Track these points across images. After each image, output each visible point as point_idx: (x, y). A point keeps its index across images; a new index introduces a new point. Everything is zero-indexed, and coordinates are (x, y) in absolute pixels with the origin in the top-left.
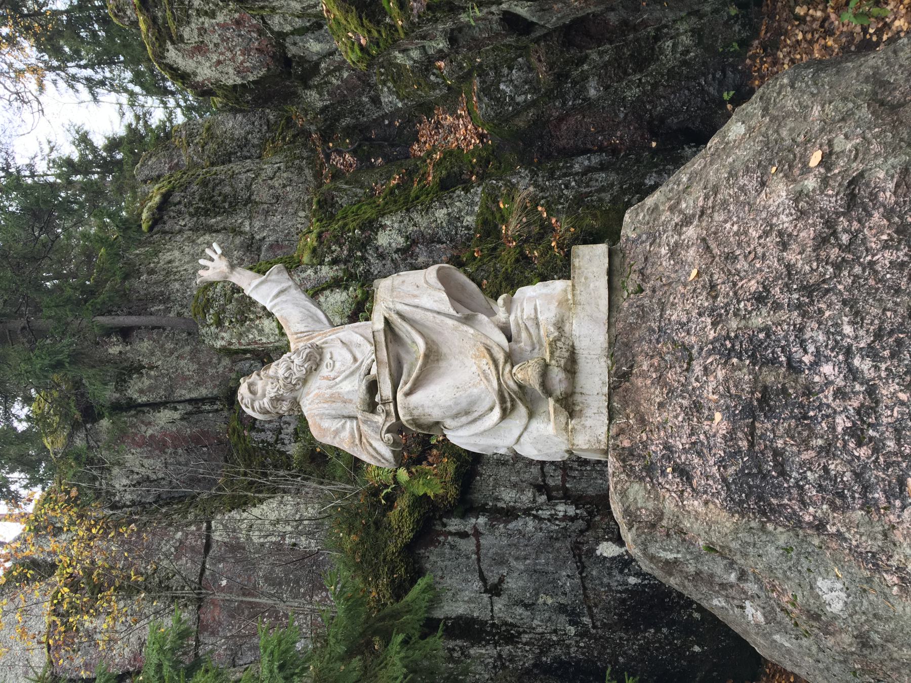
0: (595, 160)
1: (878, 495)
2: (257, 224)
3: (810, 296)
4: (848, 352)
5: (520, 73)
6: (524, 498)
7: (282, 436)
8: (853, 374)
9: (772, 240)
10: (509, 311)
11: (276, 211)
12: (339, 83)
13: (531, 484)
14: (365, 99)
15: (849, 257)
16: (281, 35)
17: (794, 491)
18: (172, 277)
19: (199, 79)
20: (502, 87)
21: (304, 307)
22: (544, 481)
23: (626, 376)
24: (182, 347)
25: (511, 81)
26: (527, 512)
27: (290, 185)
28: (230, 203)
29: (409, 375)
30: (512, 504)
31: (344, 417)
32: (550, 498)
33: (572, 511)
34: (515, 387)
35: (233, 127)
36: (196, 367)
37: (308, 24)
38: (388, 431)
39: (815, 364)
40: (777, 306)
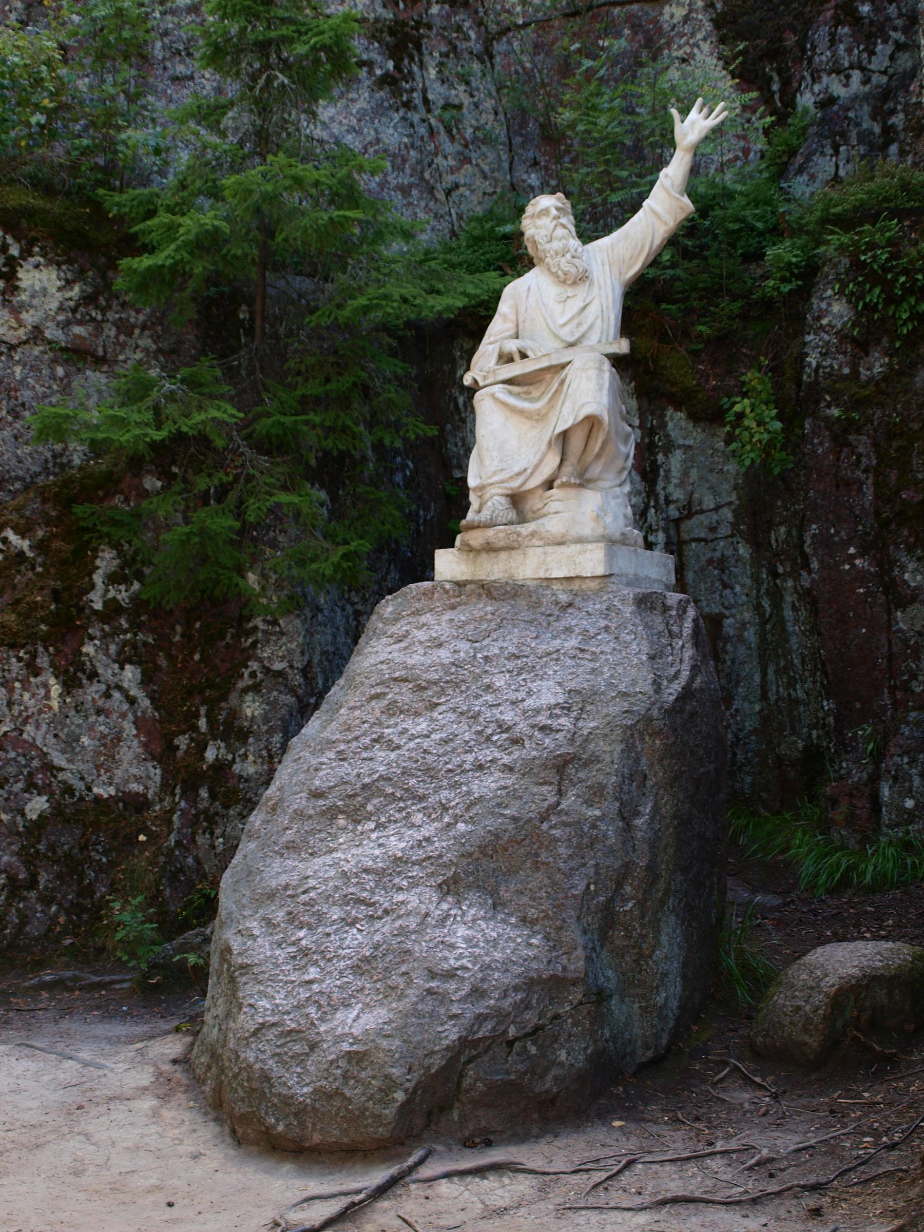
1: (342, 747)
3: (472, 717)
6: (671, 488)
7: (825, 79)
8: (412, 738)
9: (520, 695)
17: (359, 704)
21: (643, 247)
22: (697, 513)
23: (490, 596)
26: (651, 492)
29: (518, 395)
30: (662, 472)
32: (677, 522)
40: (477, 697)
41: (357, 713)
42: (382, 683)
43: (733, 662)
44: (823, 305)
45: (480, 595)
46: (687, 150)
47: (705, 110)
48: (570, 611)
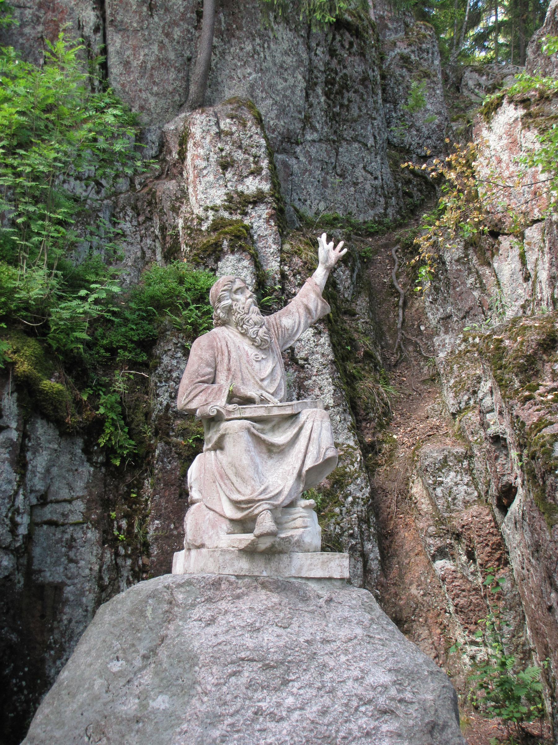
0: (374, 565)
1: (230, 720)
2: (313, 151)
3: (329, 692)
4: (302, 709)
5: (463, 493)
6: (36, 480)
10: (306, 507)
11: (327, 173)
12: (469, 286)
13: (49, 488)
14: (449, 309)
15: (352, 710)
16: (521, 236)
18: (258, 41)
19: (485, 133)
20: (452, 474)
22: (51, 502)
24: (175, 50)
25: (457, 484)
26: (22, 483)
27: (355, 191)
28: (338, 114)
30: (30, 467)
31: (216, 367)
32: (32, 507)
33: (23, 530)
34: (256, 512)
35: (426, 111)
36: (149, 66)
37: (529, 267)
38: (218, 411)
39: (293, 694)
41: (225, 689)
42: (233, 662)
43: (70, 621)
44: (174, 362)
45: (256, 588)
46: (327, 268)
47: (332, 244)
48: (332, 604)
